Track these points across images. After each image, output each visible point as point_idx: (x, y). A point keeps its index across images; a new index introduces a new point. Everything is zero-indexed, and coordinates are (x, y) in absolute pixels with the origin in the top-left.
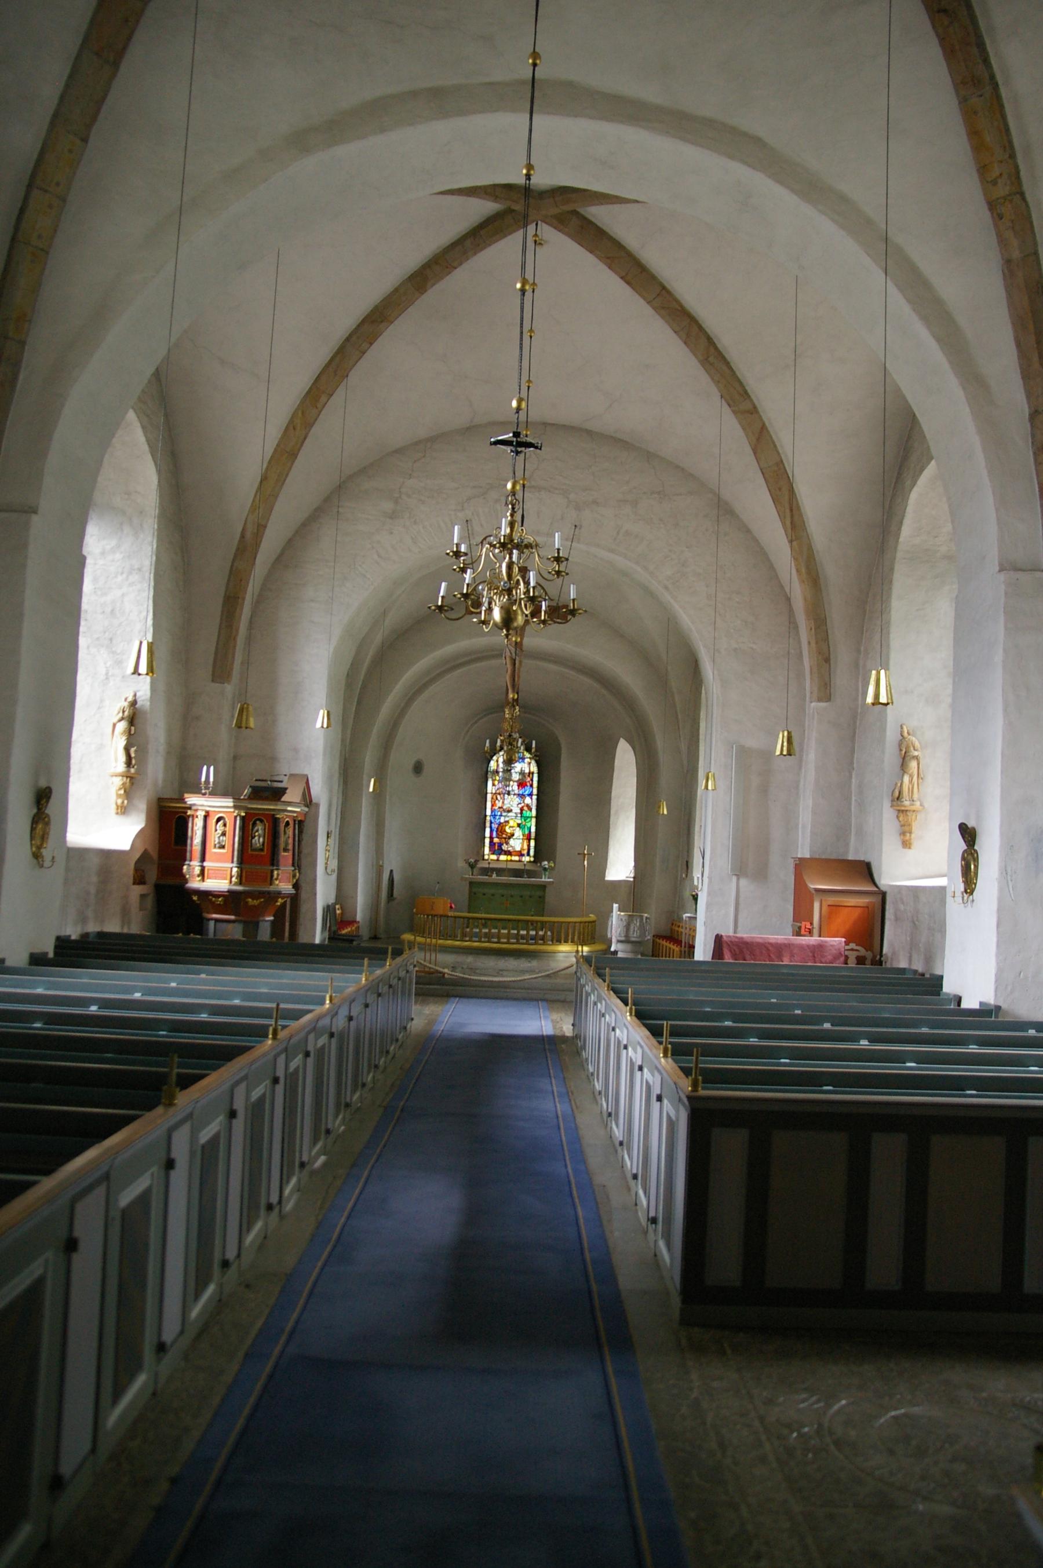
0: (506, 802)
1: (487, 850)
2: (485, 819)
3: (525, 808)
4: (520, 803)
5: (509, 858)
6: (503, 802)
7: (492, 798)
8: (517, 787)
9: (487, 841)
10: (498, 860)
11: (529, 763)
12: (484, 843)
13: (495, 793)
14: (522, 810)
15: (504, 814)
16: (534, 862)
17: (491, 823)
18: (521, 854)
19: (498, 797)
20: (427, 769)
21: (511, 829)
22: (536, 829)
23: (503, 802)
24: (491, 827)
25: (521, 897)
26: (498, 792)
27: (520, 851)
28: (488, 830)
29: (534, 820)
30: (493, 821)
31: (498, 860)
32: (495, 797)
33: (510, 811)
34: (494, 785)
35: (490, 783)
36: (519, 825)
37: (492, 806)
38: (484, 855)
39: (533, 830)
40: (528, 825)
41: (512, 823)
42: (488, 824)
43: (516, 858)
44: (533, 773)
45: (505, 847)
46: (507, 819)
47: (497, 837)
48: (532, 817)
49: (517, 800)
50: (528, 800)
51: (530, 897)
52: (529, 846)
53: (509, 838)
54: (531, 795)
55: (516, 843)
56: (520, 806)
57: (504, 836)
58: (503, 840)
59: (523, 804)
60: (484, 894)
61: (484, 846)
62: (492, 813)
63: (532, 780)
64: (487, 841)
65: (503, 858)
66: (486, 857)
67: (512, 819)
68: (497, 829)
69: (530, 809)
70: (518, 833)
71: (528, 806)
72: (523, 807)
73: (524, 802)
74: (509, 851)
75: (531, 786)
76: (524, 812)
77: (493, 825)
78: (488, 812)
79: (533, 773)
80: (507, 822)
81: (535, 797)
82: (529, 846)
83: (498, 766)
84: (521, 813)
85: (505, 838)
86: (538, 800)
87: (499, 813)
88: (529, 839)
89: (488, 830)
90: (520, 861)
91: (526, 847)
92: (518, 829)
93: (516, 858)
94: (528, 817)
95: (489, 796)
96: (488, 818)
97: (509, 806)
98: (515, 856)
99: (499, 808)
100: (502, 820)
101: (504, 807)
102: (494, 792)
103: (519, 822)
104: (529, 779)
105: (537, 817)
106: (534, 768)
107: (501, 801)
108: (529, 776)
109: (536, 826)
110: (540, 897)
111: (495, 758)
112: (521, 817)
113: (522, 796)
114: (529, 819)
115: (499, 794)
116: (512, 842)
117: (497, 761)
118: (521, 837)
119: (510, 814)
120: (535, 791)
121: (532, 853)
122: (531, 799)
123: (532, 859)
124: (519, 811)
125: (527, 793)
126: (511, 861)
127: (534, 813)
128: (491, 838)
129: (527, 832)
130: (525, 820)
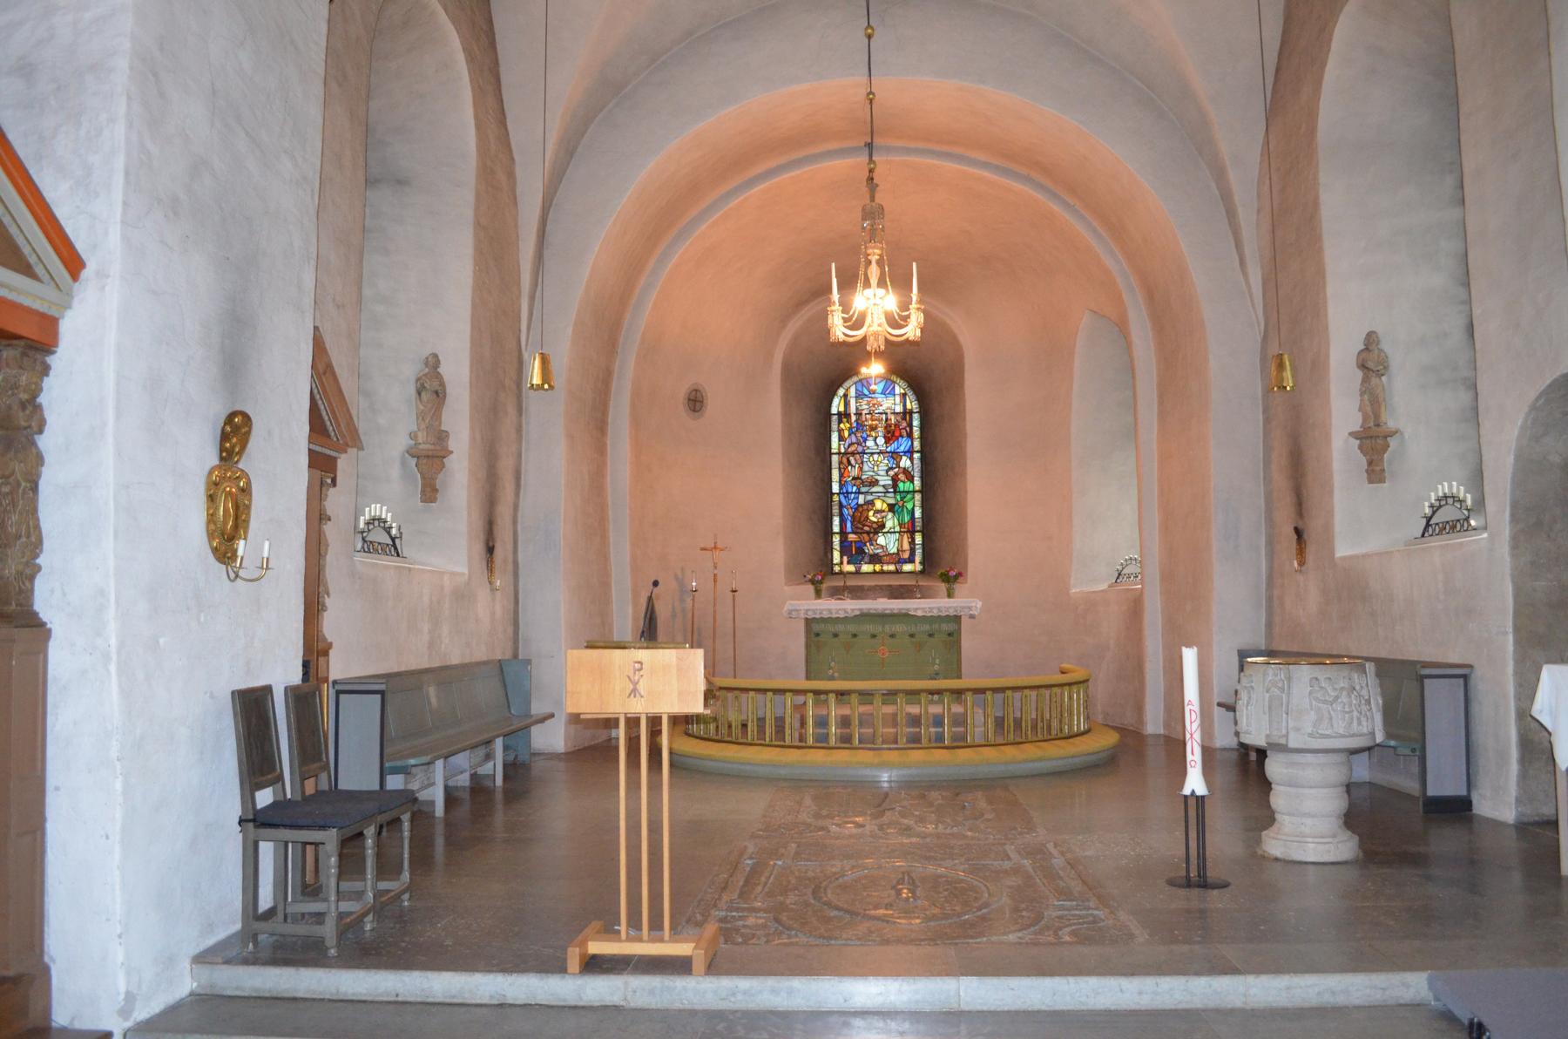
0: (866, 468)
1: (836, 556)
2: (832, 501)
3: (902, 477)
4: (891, 468)
5: (878, 567)
6: (861, 469)
7: (840, 463)
8: (883, 441)
9: (836, 539)
10: (858, 572)
11: (904, 395)
12: (832, 542)
13: (845, 453)
14: (895, 480)
15: (864, 489)
16: (922, 572)
17: (841, 506)
18: (898, 559)
19: (852, 459)
20: (712, 405)
21: (879, 516)
22: (923, 513)
23: (861, 469)
24: (841, 515)
25: (912, 636)
26: (850, 450)
27: (898, 554)
28: (836, 521)
29: (918, 497)
30: (844, 503)
31: (858, 572)
32: (845, 460)
33: (875, 483)
34: (841, 438)
35: (835, 437)
36: (891, 508)
37: (841, 476)
38: (832, 564)
39: (918, 514)
40: (909, 506)
41: (879, 505)
42: (836, 510)
43: (892, 568)
44: (911, 412)
45: (869, 549)
46: (869, 498)
47: (853, 533)
48: (914, 492)
49: (884, 463)
50: (905, 462)
51: (931, 635)
52: (912, 542)
53: (876, 533)
54: (910, 452)
55: (888, 542)
56: (891, 473)
57: (866, 528)
58: (865, 535)
59: (896, 470)
60: (836, 635)
61: (832, 548)
62: (841, 488)
63: (910, 425)
64: (836, 539)
65: (866, 568)
66: (837, 569)
67: (879, 498)
68: (853, 517)
69: (911, 479)
70: (891, 522)
71: (905, 471)
72: (896, 474)
73: (898, 466)
74: (877, 554)
75: (910, 435)
76: (901, 485)
77: (845, 511)
78: (835, 488)
79: (911, 412)
80: (871, 503)
81: (916, 456)
82: (912, 542)
83: (847, 404)
84: (895, 485)
85: (868, 533)
86: (922, 459)
87: (855, 489)
88: (912, 532)
89: (836, 521)
90: (898, 572)
91: (906, 546)
92: (890, 515)
93: (892, 568)
94: (908, 492)
95: (835, 459)
96: (836, 498)
97: (871, 473)
98: (888, 563)
99: (854, 479)
100: (861, 500)
101: (863, 477)
102: (843, 450)
103: (892, 501)
104: (904, 424)
105: (924, 491)
106: (912, 404)
107: (857, 466)
108: (904, 419)
109: (923, 507)
110: (950, 634)
111: (841, 392)
112: (895, 492)
113: (895, 456)
114: (909, 496)
115: (853, 454)
116: (881, 540)
117: (845, 396)
118: (897, 529)
119: (875, 489)
120: (917, 445)
121: (918, 558)
122: (911, 459)
123: (919, 567)
124: (890, 482)
125: (902, 449)
126: (882, 572)
127: (917, 483)
128: (843, 533)
129: (907, 519)
130: (902, 499)
